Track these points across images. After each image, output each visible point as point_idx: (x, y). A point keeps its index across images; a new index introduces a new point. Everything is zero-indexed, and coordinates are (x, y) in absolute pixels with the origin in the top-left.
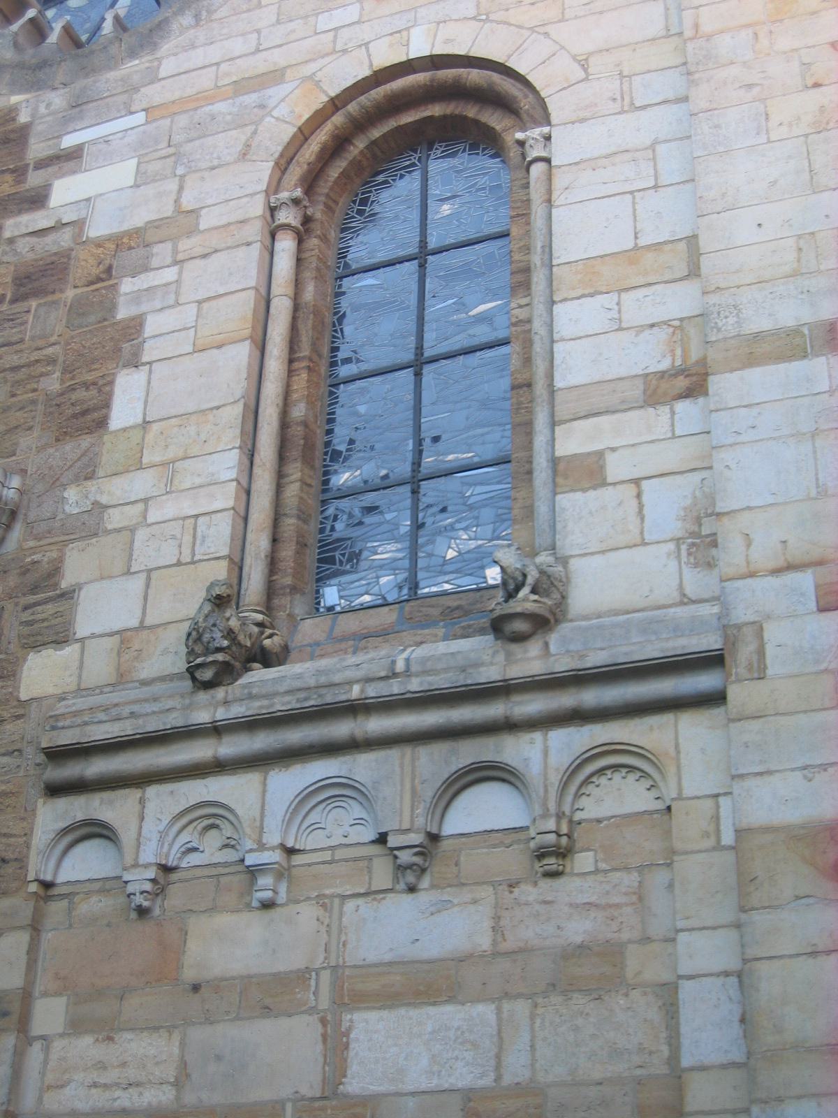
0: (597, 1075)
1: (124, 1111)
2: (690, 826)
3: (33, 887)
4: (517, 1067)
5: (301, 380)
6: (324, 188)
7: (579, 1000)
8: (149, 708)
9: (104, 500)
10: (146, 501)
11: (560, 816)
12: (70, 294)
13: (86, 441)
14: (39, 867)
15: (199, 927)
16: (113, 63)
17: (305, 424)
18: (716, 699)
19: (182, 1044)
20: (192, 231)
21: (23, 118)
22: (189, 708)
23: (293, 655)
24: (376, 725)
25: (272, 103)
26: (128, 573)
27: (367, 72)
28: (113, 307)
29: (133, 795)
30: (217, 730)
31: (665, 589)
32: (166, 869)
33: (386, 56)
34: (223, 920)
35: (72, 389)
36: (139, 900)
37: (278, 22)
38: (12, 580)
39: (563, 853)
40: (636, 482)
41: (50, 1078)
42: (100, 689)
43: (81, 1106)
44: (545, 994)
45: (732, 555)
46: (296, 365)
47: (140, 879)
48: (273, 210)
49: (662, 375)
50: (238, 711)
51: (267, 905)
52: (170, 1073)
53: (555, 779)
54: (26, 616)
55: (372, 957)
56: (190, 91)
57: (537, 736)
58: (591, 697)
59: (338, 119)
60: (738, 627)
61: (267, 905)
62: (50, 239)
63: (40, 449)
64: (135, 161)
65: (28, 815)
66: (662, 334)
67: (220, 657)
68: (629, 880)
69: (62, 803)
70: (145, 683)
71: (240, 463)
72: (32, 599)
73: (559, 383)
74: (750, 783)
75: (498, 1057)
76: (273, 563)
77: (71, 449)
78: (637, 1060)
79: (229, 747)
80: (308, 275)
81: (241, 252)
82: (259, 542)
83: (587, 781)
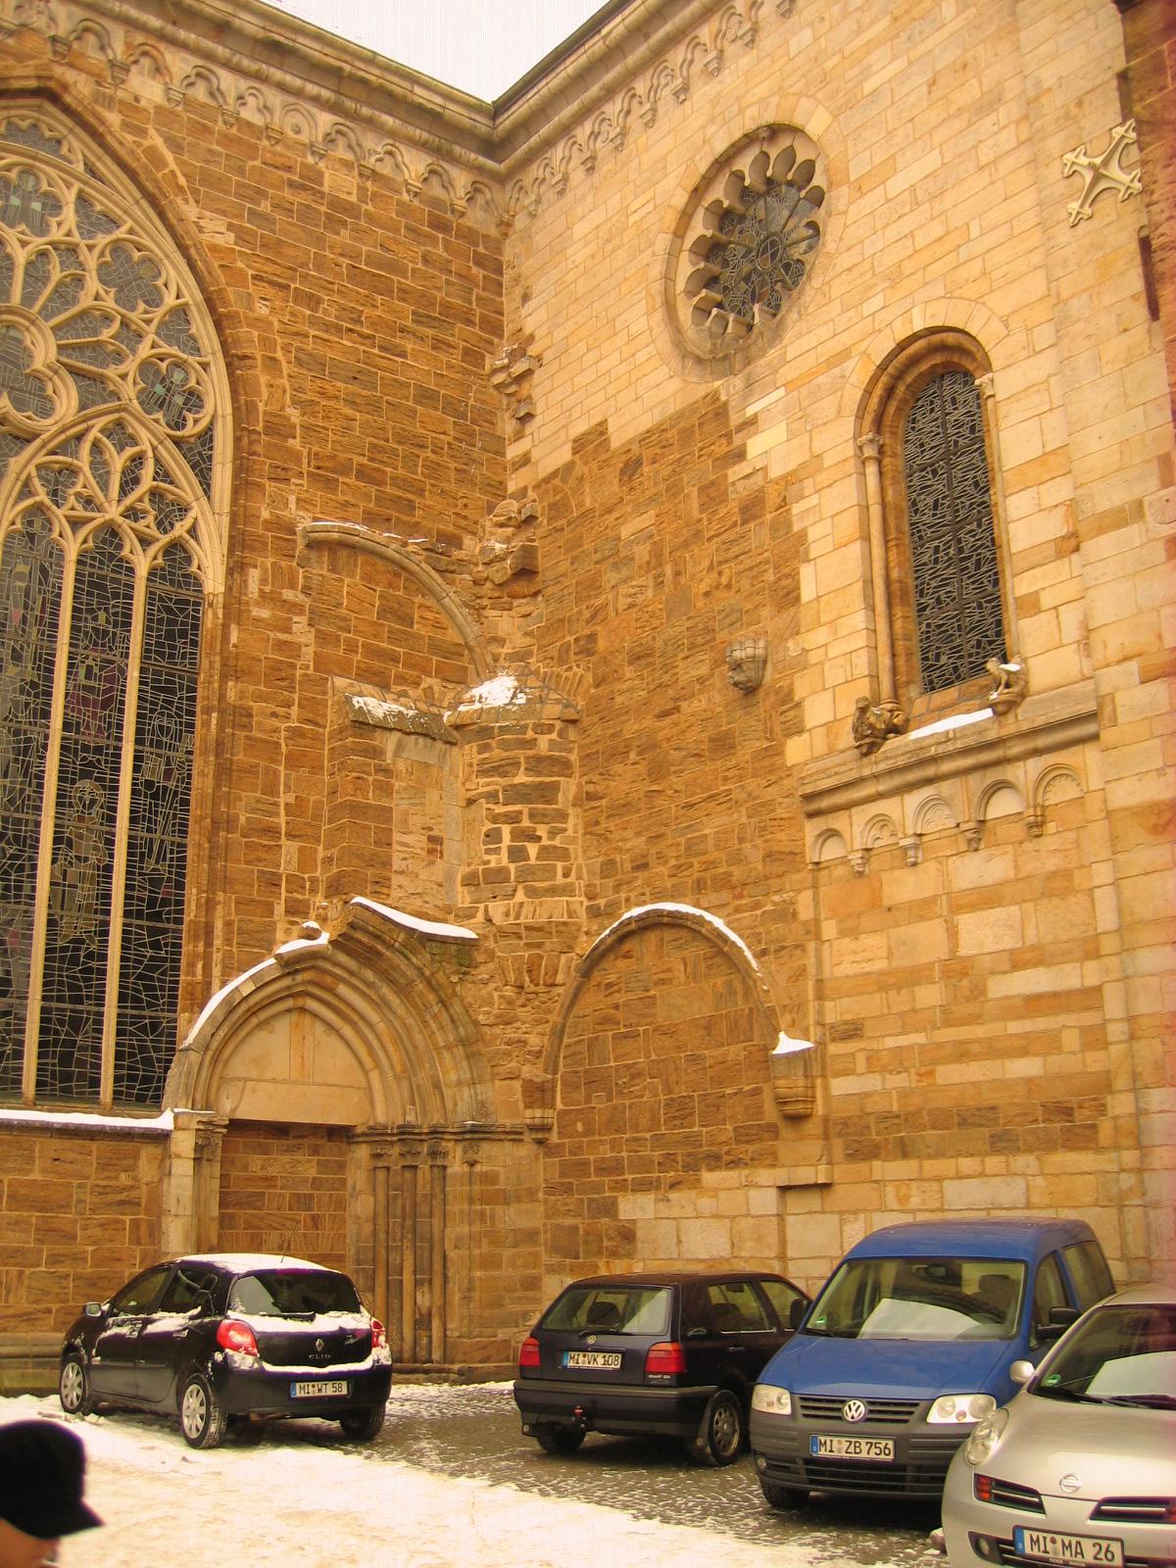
0: (1066, 938)
1: (868, 973)
2: (1094, 807)
3: (810, 867)
4: (1031, 938)
5: (893, 554)
6: (887, 421)
7: (1056, 901)
8: (843, 769)
9: (807, 647)
10: (826, 645)
11: (1035, 806)
12: (769, 516)
13: (792, 610)
14: (812, 856)
15: (885, 876)
16: (763, 353)
17: (900, 581)
18: (1095, 737)
19: (888, 938)
20: (821, 469)
21: (723, 398)
22: (860, 767)
23: (912, 723)
24: (947, 767)
25: (847, 374)
26: (824, 689)
27: (893, 346)
28: (789, 525)
29: (846, 813)
30: (876, 777)
31: (1075, 674)
32: (868, 850)
33: (902, 333)
34: (897, 873)
35: (780, 579)
36: (857, 868)
37: (843, 312)
38: (772, 698)
39: (1040, 825)
40: (1055, 608)
41: (835, 960)
42: (821, 758)
43: (850, 973)
44: (1039, 898)
45: (1099, 655)
46: (890, 544)
47: (856, 858)
48: (860, 448)
49: (1063, 538)
50: (883, 766)
51: (914, 864)
52: (884, 953)
53: (1031, 786)
54: (782, 719)
55: (963, 886)
56: (805, 369)
57: (1021, 764)
58: (1041, 742)
59: (884, 379)
60: (1103, 697)
61: (914, 864)
62: (753, 479)
63: (772, 618)
64: (784, 424)
65: (802, 829)
66: (1061, 511)
67: (868, 740)
68: (1072, 835)
69: (815, 821)
70: (842, 752)
71: (867, 616)
72: (784, 708)
73: (1014, 551)
74: (1114, 784)
75: (1023, 933)
76: (894, 670)
77: (786, 616)
78: (1083, 928)
79: (882, 787)
80: (888, 482)
81: (847, 481)
82: (885, 661)
83: (1048, 784)
